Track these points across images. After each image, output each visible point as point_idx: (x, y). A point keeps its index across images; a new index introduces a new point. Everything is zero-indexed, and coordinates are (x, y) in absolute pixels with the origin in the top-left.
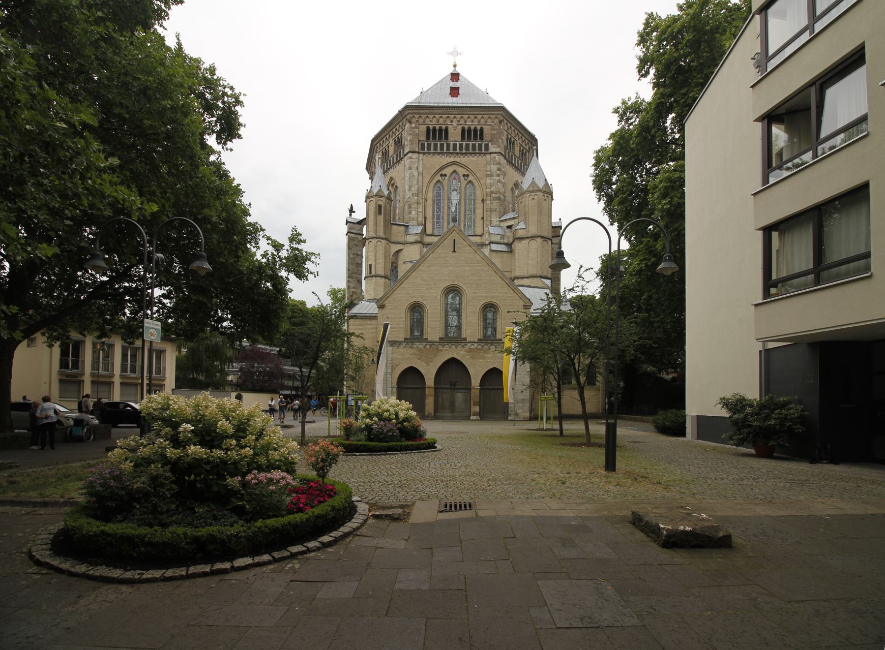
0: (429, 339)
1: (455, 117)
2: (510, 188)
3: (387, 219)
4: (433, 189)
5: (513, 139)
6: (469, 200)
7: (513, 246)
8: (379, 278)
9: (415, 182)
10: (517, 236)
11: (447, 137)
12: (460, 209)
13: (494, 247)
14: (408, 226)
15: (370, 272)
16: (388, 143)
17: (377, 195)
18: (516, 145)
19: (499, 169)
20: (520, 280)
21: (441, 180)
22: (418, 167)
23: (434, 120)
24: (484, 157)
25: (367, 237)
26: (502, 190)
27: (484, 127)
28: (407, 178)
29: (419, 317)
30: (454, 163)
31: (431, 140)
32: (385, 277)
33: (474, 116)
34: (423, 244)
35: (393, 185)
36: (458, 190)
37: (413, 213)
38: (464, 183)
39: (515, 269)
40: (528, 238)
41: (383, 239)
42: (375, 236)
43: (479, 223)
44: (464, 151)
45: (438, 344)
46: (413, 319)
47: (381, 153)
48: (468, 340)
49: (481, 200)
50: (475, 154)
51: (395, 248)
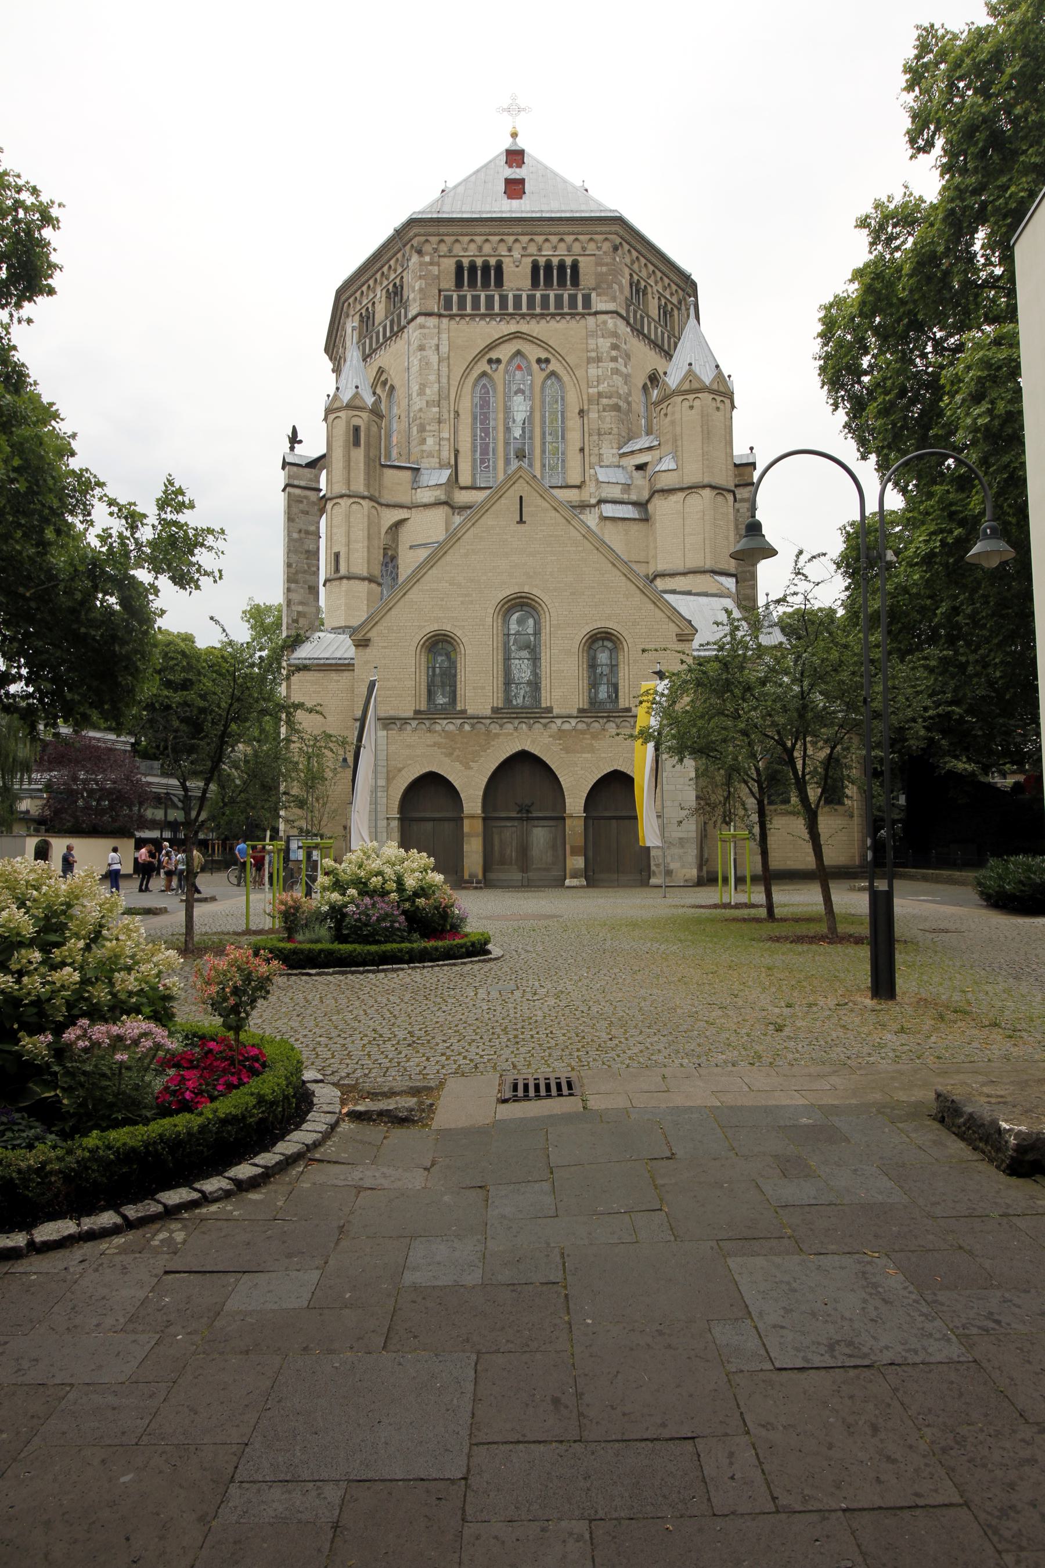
0: (469, 711)
1: (516, 240)
2: (640, 385)
3: (371, 454)
4: (473, 392)
5: (643, 284)
6: (551, 413)
7: (650, 507)
8: (357, 582)
9: (433, 378)
10: (658, 487)
11: (499, 282)
12: (532, 431)
13: (608, 510)
14: (419, 469)
15: (337, 570)
16: (371, 296)
17: (349, 406)
18: (650, 296)
19: (615, 347)
20: (667, 579)
21: (489, 371)
22: (438, 346)
23: (473, 246)
24: (583, 321)
25: (329, 495)
26: (623, 390)
27: (580, 259)
28: (414, 369)
29: (446, 664)
30: (517, 336)
31: (466, 288)
32: (370, 579)
33: (559, 237)
34: (452, 507)
35: (385, 383)
36: (527, 393)
37: (430, 441)
38: (539, 376)
39: (655, 557)
40: (682, 489)
41: (364, 498)
42: (347, 492)
43: (574, 460)
44: (538, 310)
45: (488, 721)
46: (434, 668)
47: (357, 317)
48: (556, 711)
49: (577, 411)
50: (563, 315)
51: (391, 516)
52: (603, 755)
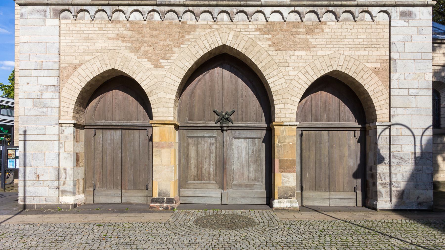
45: (183, 9)
52: (320, 53)
